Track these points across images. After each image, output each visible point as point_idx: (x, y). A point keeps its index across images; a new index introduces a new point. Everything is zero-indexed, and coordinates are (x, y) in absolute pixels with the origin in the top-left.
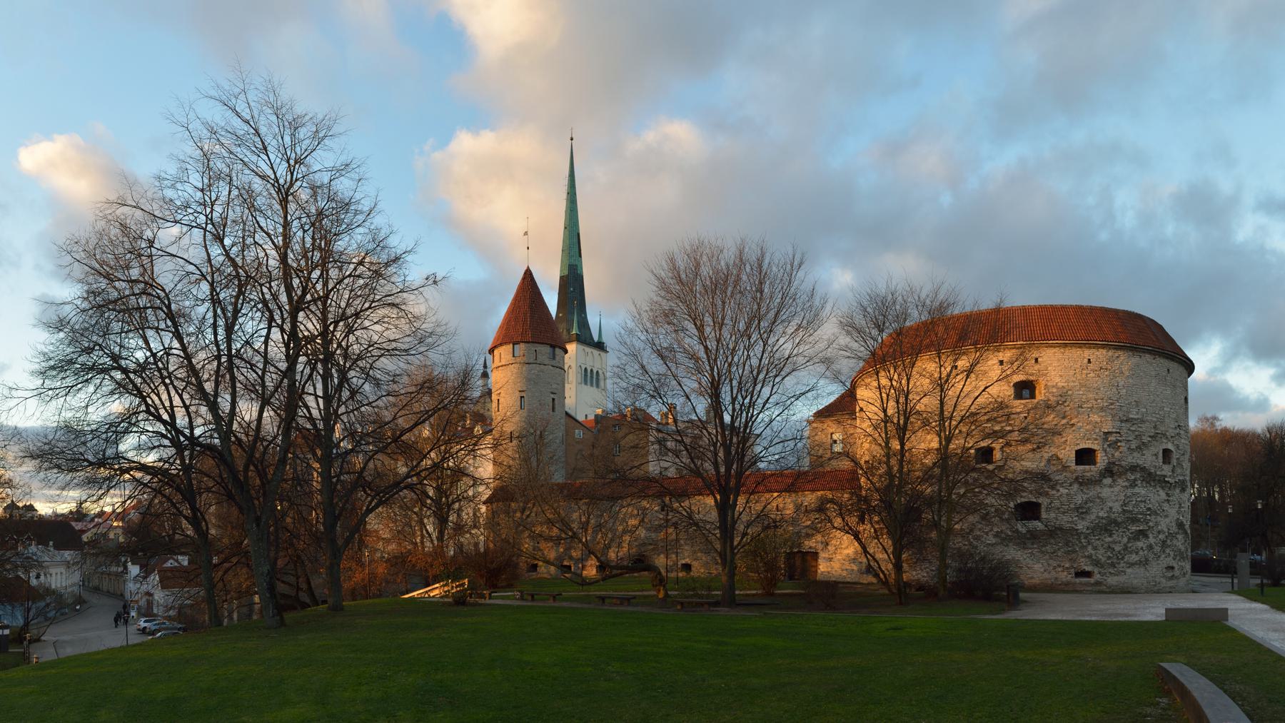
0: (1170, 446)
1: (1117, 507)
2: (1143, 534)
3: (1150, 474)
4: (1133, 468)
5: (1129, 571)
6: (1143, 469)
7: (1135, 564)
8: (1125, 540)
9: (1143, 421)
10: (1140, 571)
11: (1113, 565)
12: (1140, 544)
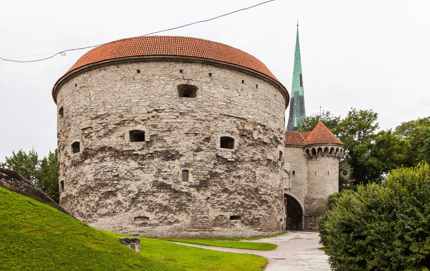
0: (139, 127)
1: (90, 177)
2: (113, 194)
3: (117, 151)
4: (103, 149)
5: (100, 219)
6: (110, 148)
7: (105, 215)
8: (97, 199)
9: (109, 115)
10: (108, 219)
11: (90, 216)
12: (108, 201)
